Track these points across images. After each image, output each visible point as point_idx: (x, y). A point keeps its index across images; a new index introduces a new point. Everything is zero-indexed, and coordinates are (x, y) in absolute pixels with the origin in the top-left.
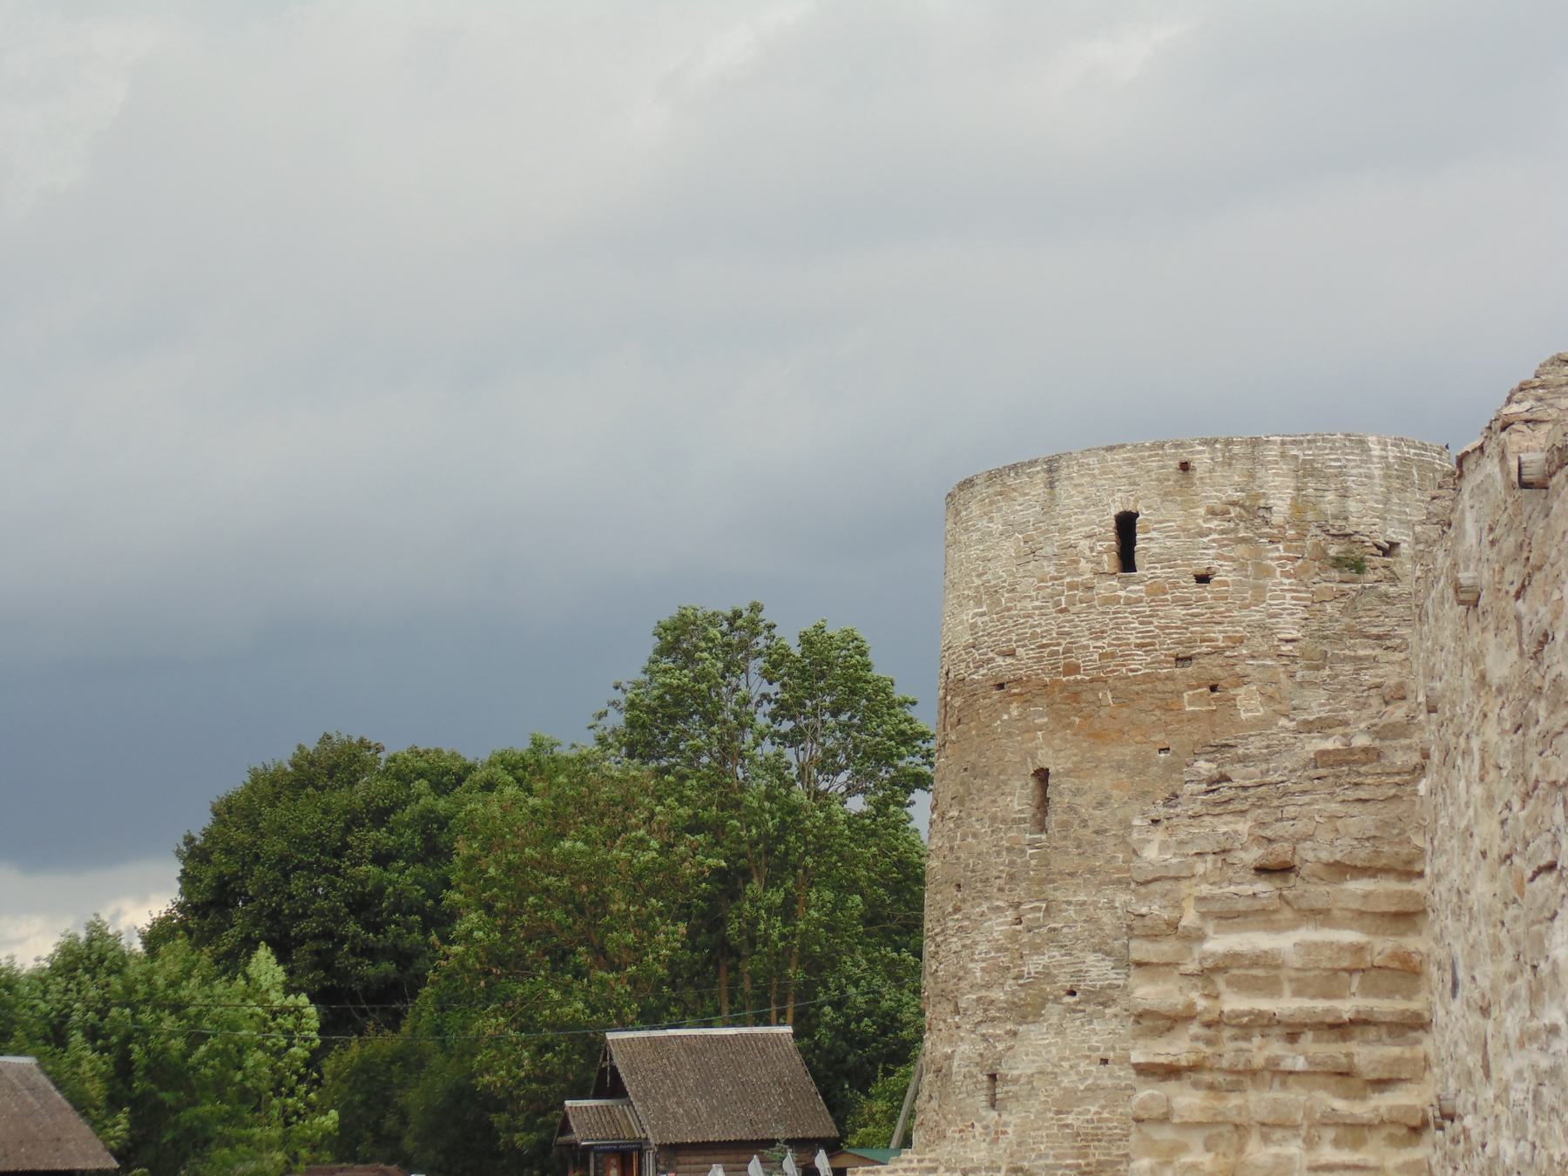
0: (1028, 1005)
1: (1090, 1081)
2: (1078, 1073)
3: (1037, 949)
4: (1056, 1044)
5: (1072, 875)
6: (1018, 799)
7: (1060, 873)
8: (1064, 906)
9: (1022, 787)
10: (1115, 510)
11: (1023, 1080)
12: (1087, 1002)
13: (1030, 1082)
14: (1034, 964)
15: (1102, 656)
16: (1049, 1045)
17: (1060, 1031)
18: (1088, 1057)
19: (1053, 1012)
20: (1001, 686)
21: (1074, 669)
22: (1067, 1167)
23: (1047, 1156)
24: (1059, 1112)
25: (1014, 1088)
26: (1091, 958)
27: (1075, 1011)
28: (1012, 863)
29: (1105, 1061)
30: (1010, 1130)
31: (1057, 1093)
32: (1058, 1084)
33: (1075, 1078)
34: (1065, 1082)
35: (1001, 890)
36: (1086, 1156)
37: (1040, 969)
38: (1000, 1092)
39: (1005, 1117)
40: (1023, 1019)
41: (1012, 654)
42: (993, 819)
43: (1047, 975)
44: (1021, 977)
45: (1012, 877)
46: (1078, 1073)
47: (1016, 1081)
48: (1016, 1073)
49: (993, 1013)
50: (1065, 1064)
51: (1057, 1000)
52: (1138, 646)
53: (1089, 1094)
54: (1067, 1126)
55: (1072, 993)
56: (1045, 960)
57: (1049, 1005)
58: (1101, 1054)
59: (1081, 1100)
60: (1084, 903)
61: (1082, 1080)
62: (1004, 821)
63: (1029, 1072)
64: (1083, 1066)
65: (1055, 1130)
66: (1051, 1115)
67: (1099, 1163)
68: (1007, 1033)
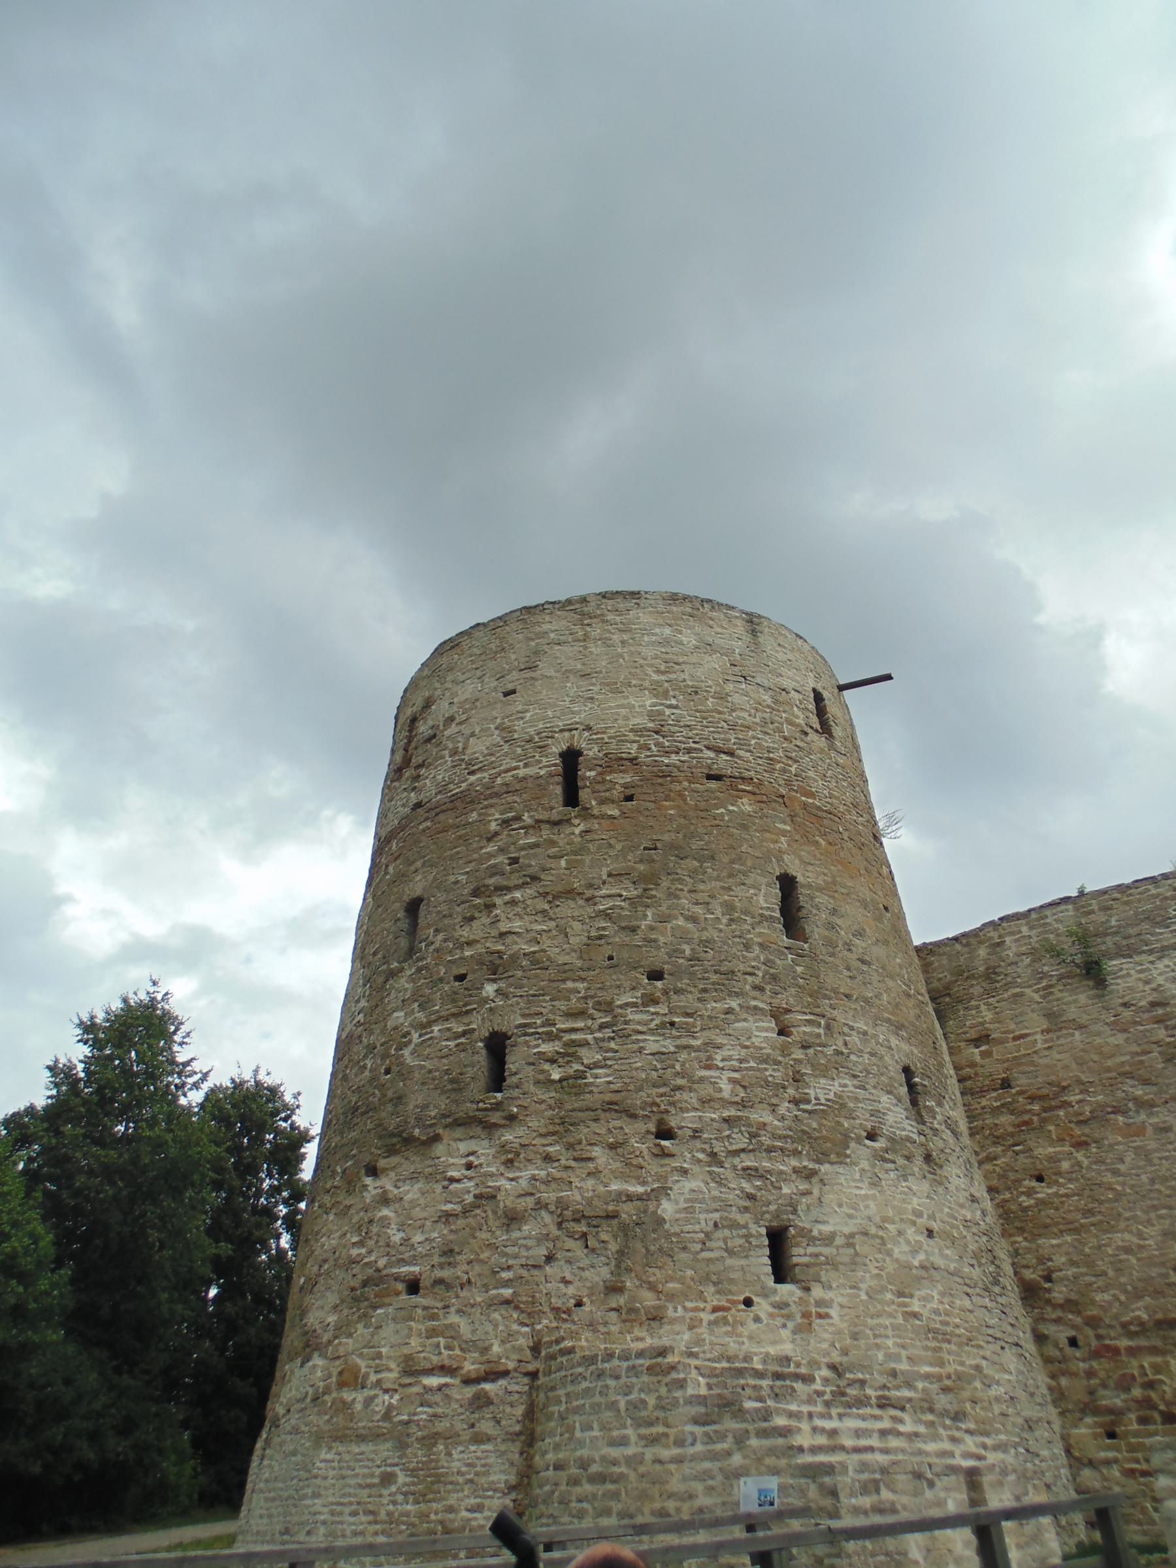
0: (826, 1139)
1: (921, 1257)
2: (908, 1242)
3: (822, 1071)
4: (874, 1198)
6: (768, 899)
7: (835, 991)
8: (846, 1029)
9: (769, 885)
11: (839, 1241)
12: (895, 1152)
13: (850, 1245)
16: (866, 1197)
17: (875, 1183)
18: (914, 1223)
19: (861, 1153)
22: (927, 1377)
23: (897, 1358)
24: (900, 1294)
25: (826, 1251)
26: (885, 1098)
27: (884, 1160)
28: (768, 963)
29: (930, 1233)
30: (833, 1312)
31: (890, 1267)
32: (889, 1253)
33: (906, 1248)
34: (899, 1251)
35: (758, 988)
36: (941, 1363)
37: (831, 1096)
38: (799, 1254)
39: (817, 1292)
40: (822, 1157)
42: (729, 907)
43: (839, 1106)
46: (908, 1242)
47: (828, 1240)
48: (826, 1229)
49: (766, 1141)
50: (891, 1228)
53: (923, 1273)
54: (915, 1315)
55: (871, 1136)
57: (852, 1145)
59: (919, 1279)
60: (865, 1033)
61: (914, 1252)
62: (746, 912)
63: (846, 1230)
64: (910, 1232)
65: (900, 1320)
66: (889, 1296)
67: (959, 1377)
68: (796, 1171)
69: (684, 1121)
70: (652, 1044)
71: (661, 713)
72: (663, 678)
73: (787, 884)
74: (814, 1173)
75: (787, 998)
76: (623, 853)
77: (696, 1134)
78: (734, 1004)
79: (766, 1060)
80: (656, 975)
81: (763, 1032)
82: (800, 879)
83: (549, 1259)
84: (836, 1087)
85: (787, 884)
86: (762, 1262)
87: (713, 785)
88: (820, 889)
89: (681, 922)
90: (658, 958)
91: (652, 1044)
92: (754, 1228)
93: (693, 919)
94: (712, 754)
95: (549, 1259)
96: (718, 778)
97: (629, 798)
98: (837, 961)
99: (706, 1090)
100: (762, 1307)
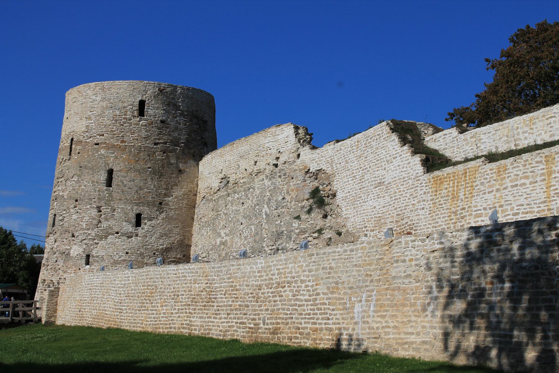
3: (107, 219)
5: (120, 200)
6: (103, 177)
10: (140, 99)
14: (104, 224)
15: (133, 139)
20: (97, 144)
21: (125, 142)
25: (97, 259)
26: (124, 224)
28: (99, 195)
29: (127, 253)
35: (95, 202)
38: (91, 260)
40: (101, 239)
41: (103, 135)
42: (93, 182)
44: (101, 227)
45: (99, 199)
47: (97, 257)
48: (98, 254)
50: (115, 253)
51: (113, 234)
52: (145, 138)
55: (117, 233)
56: (109, 223)
58: (126, 250)
60: (123, 208)
62: (97, 182)
69: (76, 234)
70: (74, 217)
71: (89, 126)
72: (91, 113)
73: (110, 172)
74: (98, 243)
75: (102, 203)
76: (77, 168)
77: (78, 236)
78: (88, 207)
79: (94, 219)
80: (76, 201)
81: (94, 212)
82: (115, 170)
83: (56, 261)
84: (109, 223)
85: (110, 172)
86: (84, 261)
87: (97, 146)
88: (120, 171)
89: (83, 187)
90: (77, 197)
91: (74, 217)
92: (84, 255)
93: (85, 186)
94: (98, 136)
95: (56, 261)
96: (97, 144)
97: (79, 153)
98: (119, 191)
99: (80, 227)
100: (82, 270)
